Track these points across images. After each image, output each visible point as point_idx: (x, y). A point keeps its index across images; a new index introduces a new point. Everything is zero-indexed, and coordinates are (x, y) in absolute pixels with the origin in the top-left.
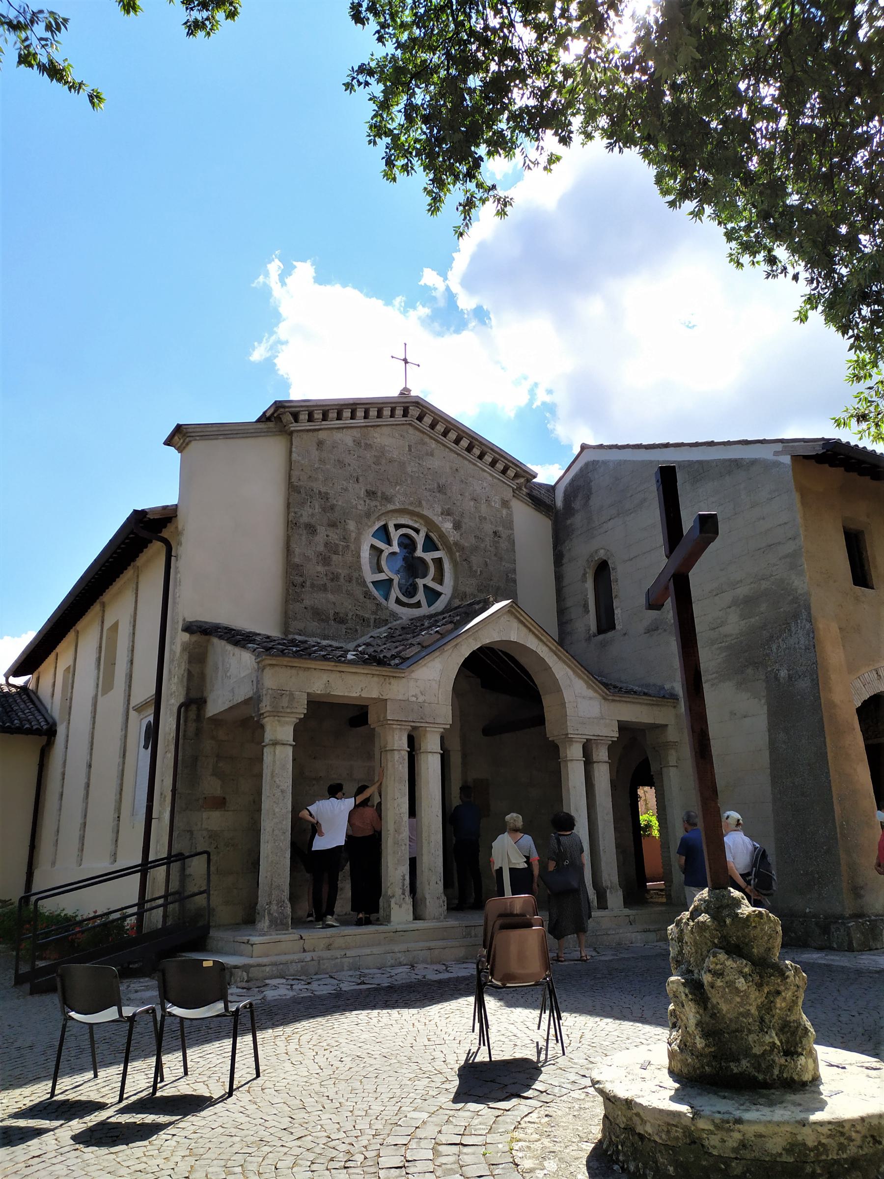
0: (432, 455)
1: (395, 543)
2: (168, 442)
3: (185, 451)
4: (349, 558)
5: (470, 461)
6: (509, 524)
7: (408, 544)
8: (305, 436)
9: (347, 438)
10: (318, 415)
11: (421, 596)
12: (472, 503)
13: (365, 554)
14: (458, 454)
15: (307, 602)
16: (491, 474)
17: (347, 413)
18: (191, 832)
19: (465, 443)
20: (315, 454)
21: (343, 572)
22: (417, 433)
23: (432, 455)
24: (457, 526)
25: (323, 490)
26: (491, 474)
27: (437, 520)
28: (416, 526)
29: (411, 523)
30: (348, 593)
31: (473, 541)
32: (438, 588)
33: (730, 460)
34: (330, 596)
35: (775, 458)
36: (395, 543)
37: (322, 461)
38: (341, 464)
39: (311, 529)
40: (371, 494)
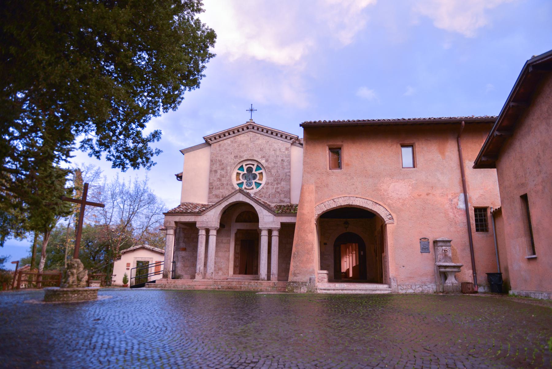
0: (259, 139)
4: (228, 178)
6: (289, 156)
7: (250, 170)
8: (215, 144)
9: (228, 141)
10: (217, 137)
11: (254, 185)
13: (234, 176)
15: (214, 193)
17: (227, 134)
18: (177, 256)
19: (270, 132)
20: (218, 149)
21: (225, 183)
23: (259, 139)
24: (267, 161)
25: (220, 159)
27: (258, 160)
30: (227, 189)
31: (273, 164)
32: (260, 182)
34: (221, 191)
37: (220, 150)
38: (226, 150)
39: (216, 171)
40: (236, 157)
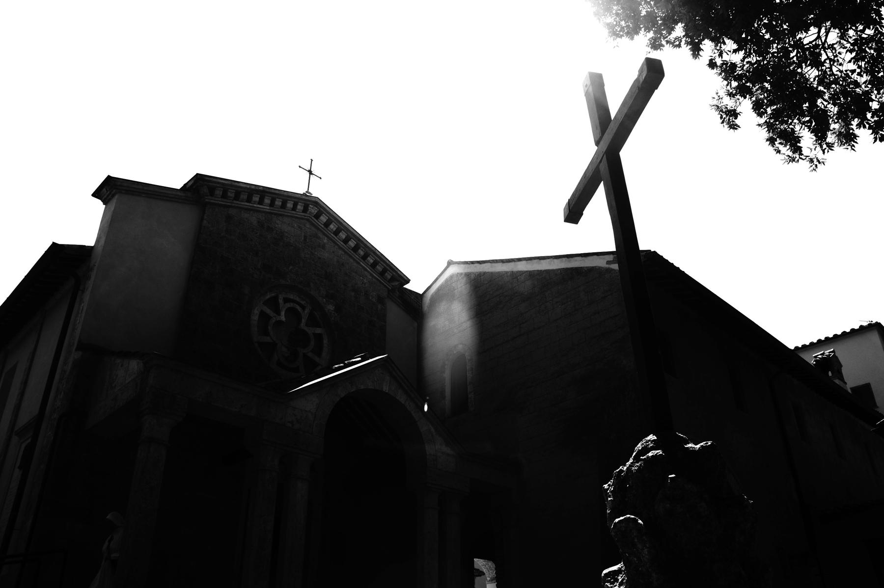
1: (283, 313)
2: (96, 194)
3: (109, 205)
5: (354, 260)
10: (231, 194)
12: (353, 294)
13: (255, 317)
14: (345, 252)
16: (371, 275)
17: (256, 198)
22: (313, 228)
26: (371, 275)
28: (303, 303)
29: (298, 299)
33: (572, 269)
35: (607, 266)
36: (283, 313)
